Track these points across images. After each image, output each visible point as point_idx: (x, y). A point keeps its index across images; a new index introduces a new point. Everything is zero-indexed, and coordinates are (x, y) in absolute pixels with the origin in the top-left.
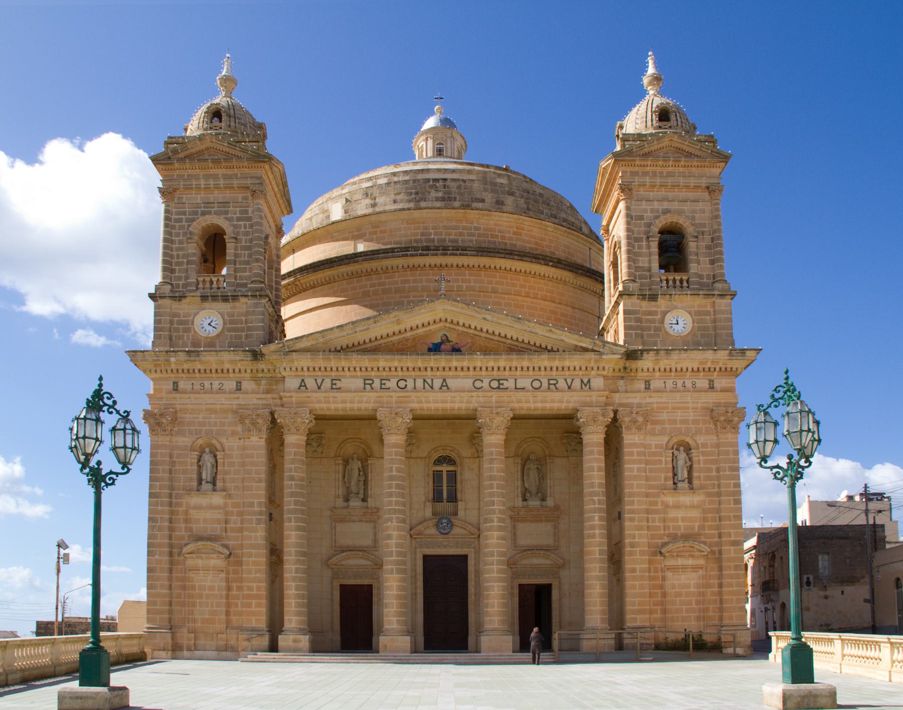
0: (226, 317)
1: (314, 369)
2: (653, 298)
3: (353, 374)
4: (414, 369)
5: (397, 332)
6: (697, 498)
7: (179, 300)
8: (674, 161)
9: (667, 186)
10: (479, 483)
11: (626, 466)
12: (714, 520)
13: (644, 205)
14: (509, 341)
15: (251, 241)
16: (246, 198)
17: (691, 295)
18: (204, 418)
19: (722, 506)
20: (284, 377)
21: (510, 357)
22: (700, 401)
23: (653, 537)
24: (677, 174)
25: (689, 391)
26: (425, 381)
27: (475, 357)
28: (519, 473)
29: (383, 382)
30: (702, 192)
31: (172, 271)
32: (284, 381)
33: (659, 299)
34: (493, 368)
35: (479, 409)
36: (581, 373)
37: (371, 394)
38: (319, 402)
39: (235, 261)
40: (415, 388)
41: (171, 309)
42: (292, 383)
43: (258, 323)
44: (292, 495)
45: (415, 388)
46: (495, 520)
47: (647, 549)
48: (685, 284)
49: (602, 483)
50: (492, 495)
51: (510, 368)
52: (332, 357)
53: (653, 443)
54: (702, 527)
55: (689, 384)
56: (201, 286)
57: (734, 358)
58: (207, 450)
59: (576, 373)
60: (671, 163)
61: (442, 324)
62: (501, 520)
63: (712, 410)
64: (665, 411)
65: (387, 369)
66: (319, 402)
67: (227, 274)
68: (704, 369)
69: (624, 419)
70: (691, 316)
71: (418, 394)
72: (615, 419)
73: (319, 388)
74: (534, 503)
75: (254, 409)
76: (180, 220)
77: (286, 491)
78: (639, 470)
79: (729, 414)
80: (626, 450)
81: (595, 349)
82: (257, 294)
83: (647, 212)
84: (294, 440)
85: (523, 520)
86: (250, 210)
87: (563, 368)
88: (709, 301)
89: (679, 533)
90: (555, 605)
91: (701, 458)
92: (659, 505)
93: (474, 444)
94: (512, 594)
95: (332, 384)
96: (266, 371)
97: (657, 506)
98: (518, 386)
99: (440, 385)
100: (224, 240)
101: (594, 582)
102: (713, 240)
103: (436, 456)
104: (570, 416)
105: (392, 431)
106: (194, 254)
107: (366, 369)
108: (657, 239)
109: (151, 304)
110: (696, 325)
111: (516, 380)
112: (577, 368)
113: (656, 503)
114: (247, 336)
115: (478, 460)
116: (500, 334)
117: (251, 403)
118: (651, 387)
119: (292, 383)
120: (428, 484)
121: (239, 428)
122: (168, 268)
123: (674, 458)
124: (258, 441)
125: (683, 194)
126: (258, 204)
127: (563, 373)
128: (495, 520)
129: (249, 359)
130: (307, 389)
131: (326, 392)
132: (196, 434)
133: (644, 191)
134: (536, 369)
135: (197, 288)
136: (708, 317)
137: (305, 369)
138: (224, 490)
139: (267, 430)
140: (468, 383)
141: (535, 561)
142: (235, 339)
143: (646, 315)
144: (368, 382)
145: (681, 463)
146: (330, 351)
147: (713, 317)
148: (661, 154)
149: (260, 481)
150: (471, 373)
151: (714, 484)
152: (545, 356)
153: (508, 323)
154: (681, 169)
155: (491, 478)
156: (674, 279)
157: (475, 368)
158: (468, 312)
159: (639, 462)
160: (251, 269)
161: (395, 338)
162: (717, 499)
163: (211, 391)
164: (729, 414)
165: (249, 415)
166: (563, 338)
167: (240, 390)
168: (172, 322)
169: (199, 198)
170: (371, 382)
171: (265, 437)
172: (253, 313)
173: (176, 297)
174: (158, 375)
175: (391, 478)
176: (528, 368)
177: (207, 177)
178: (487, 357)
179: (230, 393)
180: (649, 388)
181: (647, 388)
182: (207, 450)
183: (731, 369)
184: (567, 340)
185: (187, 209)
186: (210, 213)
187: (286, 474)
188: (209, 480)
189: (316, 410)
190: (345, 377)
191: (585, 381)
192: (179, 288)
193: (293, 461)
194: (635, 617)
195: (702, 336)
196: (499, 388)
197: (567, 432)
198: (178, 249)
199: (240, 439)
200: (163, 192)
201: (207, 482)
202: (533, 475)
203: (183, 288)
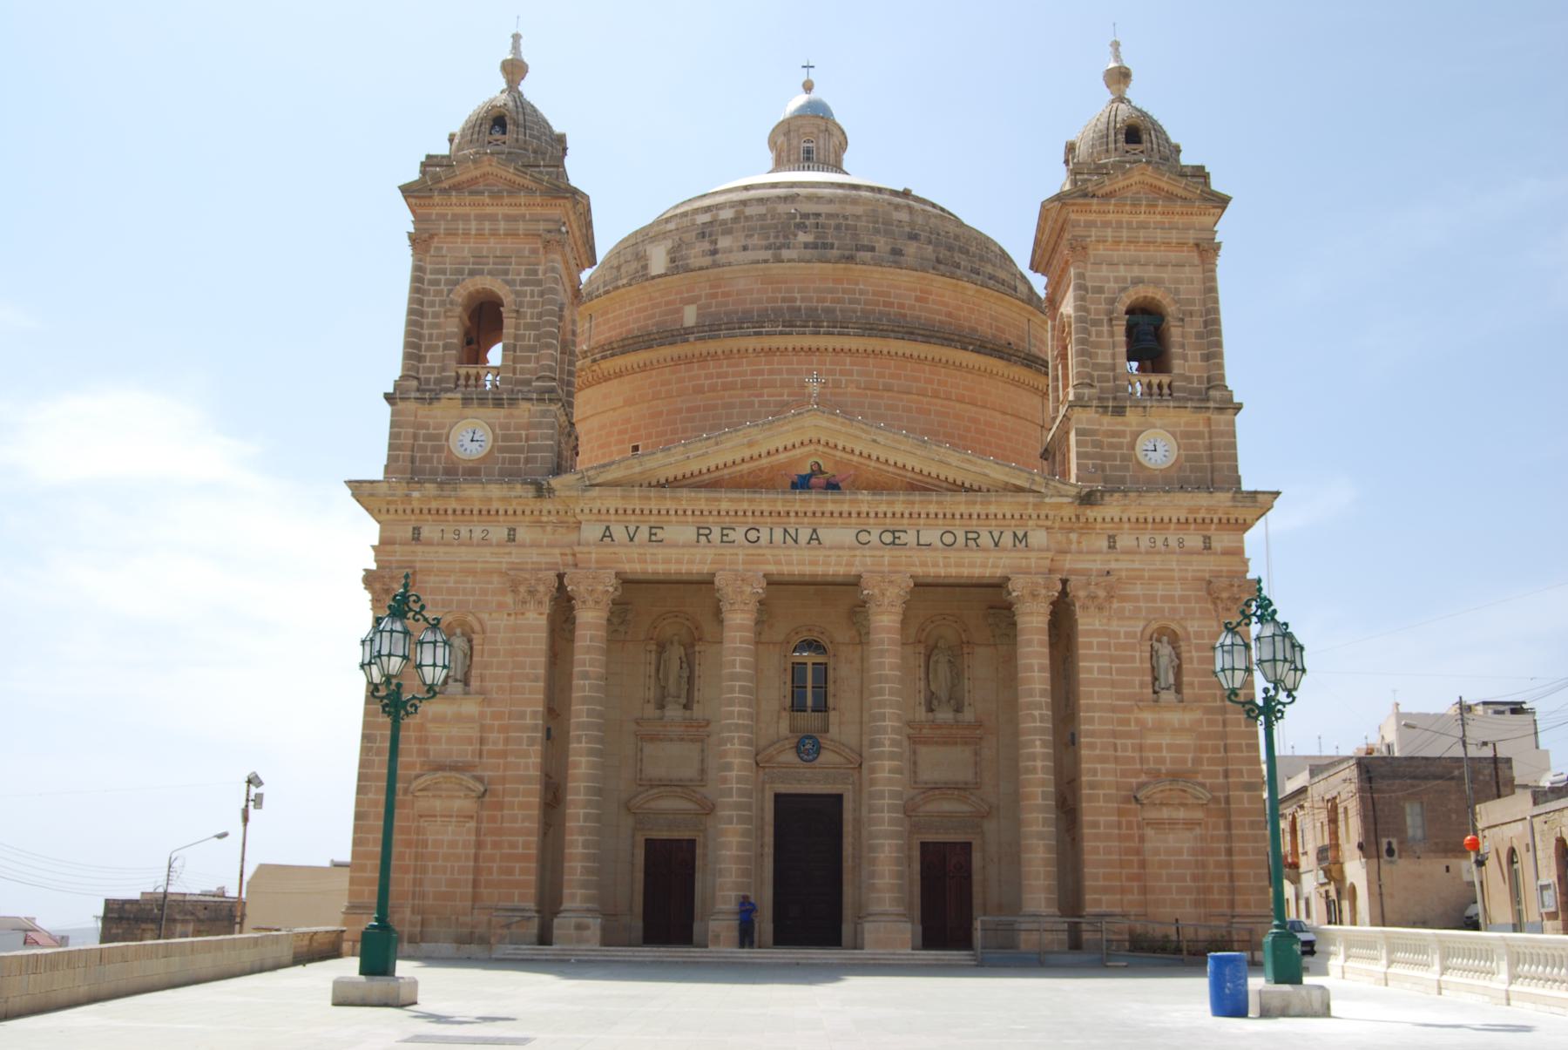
0: (498, 431)
1: (625, 511)
2: (1119, 411)
3: (683, 519)
4: (771, 513)
5: (747, 457)
6: (1188, 718)
7: (430, 404)
8: (1147, 206)
9: (1138, 242)
10: (862, 683)
11: (1081, 664)
12: (1216, 749)
13: (1105, 271)
14: (909, 474)
15: (540, 315)
16: (534, 251)
17: (1175, 407)
18: (456, 582)
19: (1228, 729)
20: (580, 523)
21: (911, 498)
22: (1190, 568)
23: (1124, 774)
24: (1152, 225)
25: (1173, 553)
26: (785, 531)
27: (860, 497)
28: (922, 669)
29: (725, 532)
30: (1189, 251)
31: (420, 359)
32: (580, 528)
33: (1127, 414)
34: (885, 514)
35: (865, 575)
36: (1013, 522)
37: (708, 551)
38: (630, 561)
39: (515, 346)
40: (771, 542)
41: (416, 416)
42: (592, 532)
43: (545, 439)
44: (585, 700)
45: (771, 542)
46: (887, 743)
47: (1114, 791)
48: (1166, 391)
49: (1046, 690)
50: (881, 704)
51: (911, 514)
52: (652, 495)
53: (1122, 630)
54: (1198, 761)
55: (1173, 542)
56: (462, 382)
57: (1240, 504)
58: (458, 631)
59: (1007, 522)
60: (1143, 209)
61: (811, 448)
62: (894, 743)
63: (1210, 582)
64: (1138, 582)
65: (732, 513)
66: (630, 561)
67: (502, 365)
68: (1195, 520)
69: (1079, 593)
70: (1175, 439)
71: (776, 552)
72: (1064, 593)
73: (631, 540)
74: (944, 715)
75: (532, 569)
76: (436, 282)
77: (576, 695)
78: (1101, 670)
79: (1235, 589)
80: (1080, 639)
81: (1034, 488)
82: (545, 396)
83: (1108, 281)
84: (590, 619)
85: (926, 742)
86: (541, 268)
87: (987, 516)
88: (1201, 417)
89: (1163, 769)
90: (976, 878)
91: (1195, 654)
92: (1133, 724)
93: (854, 624)
94: (910, 858)
95: (651, 534)
96: (554, 512)
97: (1130, 726)
98: (922, 542)
99: (808, 538)
100: (500, 314)
101: (1035, 841)
102: (1206, 324)
103: (796, 640)
104: (999, 585)
105: (736, 607)
106: (452, 335)
107: (702, 512)
108: (1125, 323)
109: (386, 409)
110: (1182, 452)
111: (918, 532)
112: (1008, 516)
113: (1127, 722)
114: (527, 461)
115: (859, 648)
116: (895, 463)
117: (529, 560)
118: (1118, 545)
119: (592, 532)
120: (785, 683)
121: (509, 599)
122: (414, 351)
123: (1154, 654)
124: (537, 619)
125: (1160, 255)
126: (553, 261)
127: (987, 522)
128: (887, 743)
129: (530, 495)
130: (613, 540)
131: (641, 546)
132: (443, 607)
133: (1104, 250)
134: (948, 516)
135: (457, 386)
136: (1200, 442)
137: (612, 511)
138: (481, 693)
139: (550, 601)
140: (847, 536)
141: (947, 806)
142: (510, 464)
143: (1108, 436)
144: (703, 531)
145: (1164, 661)
146: (650, 485)
147: (1207, 441)
148: (1129, 194)
149: (536, 679)
150: (854, 520)
151: (1215, 694)
152: (962, 497)
153: (908, 449)
154: (1158, 218)
155: (881, 679)
156: (1150, 382)
157: (859, 514)
158: (851, 431)
159: (1102, 658)
160: (538, 359)
161: (745, 467)
162: (1220, 718)
163: (469, 544)
164: (1235, 589)
165: (526, 579)
166: (987, 471)
167: (514, 540)
168: (415, 437)
169: (465, 249)
170: (707, 532)
171: (548, 611)
172: (539, 425)
173: (425, 399)
174: (391, 516)
175: (734, 677)
176: (936, 515)
177: (481, 218)
178: (878, 498)
179: (499, 545)
180: (1114, 547)
181: (1112, 547)
182: (458, 631)
183: (1237, 520)
184: (993, 474)
185: (448, 266)
186: (481, 272)
187: (577, 669)
188: (459, 677)
189: (626, 573)
190: (669, 522)
191: (1020, 535)
192: (429, 384)
193: (589, 650)
194: (1096, 901)
195: (1192, 470)
196: (893, 543)
197: (992, 608)
198: (432, 326)
199: (509, 615)
200: (414, 239)
201: (456, 680)
202: (943, 671)
203: (435, 384)
